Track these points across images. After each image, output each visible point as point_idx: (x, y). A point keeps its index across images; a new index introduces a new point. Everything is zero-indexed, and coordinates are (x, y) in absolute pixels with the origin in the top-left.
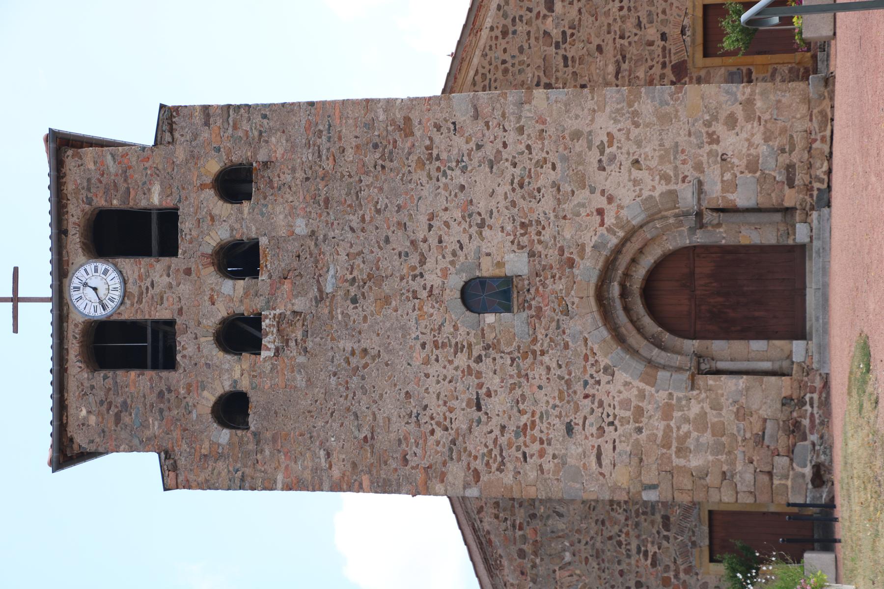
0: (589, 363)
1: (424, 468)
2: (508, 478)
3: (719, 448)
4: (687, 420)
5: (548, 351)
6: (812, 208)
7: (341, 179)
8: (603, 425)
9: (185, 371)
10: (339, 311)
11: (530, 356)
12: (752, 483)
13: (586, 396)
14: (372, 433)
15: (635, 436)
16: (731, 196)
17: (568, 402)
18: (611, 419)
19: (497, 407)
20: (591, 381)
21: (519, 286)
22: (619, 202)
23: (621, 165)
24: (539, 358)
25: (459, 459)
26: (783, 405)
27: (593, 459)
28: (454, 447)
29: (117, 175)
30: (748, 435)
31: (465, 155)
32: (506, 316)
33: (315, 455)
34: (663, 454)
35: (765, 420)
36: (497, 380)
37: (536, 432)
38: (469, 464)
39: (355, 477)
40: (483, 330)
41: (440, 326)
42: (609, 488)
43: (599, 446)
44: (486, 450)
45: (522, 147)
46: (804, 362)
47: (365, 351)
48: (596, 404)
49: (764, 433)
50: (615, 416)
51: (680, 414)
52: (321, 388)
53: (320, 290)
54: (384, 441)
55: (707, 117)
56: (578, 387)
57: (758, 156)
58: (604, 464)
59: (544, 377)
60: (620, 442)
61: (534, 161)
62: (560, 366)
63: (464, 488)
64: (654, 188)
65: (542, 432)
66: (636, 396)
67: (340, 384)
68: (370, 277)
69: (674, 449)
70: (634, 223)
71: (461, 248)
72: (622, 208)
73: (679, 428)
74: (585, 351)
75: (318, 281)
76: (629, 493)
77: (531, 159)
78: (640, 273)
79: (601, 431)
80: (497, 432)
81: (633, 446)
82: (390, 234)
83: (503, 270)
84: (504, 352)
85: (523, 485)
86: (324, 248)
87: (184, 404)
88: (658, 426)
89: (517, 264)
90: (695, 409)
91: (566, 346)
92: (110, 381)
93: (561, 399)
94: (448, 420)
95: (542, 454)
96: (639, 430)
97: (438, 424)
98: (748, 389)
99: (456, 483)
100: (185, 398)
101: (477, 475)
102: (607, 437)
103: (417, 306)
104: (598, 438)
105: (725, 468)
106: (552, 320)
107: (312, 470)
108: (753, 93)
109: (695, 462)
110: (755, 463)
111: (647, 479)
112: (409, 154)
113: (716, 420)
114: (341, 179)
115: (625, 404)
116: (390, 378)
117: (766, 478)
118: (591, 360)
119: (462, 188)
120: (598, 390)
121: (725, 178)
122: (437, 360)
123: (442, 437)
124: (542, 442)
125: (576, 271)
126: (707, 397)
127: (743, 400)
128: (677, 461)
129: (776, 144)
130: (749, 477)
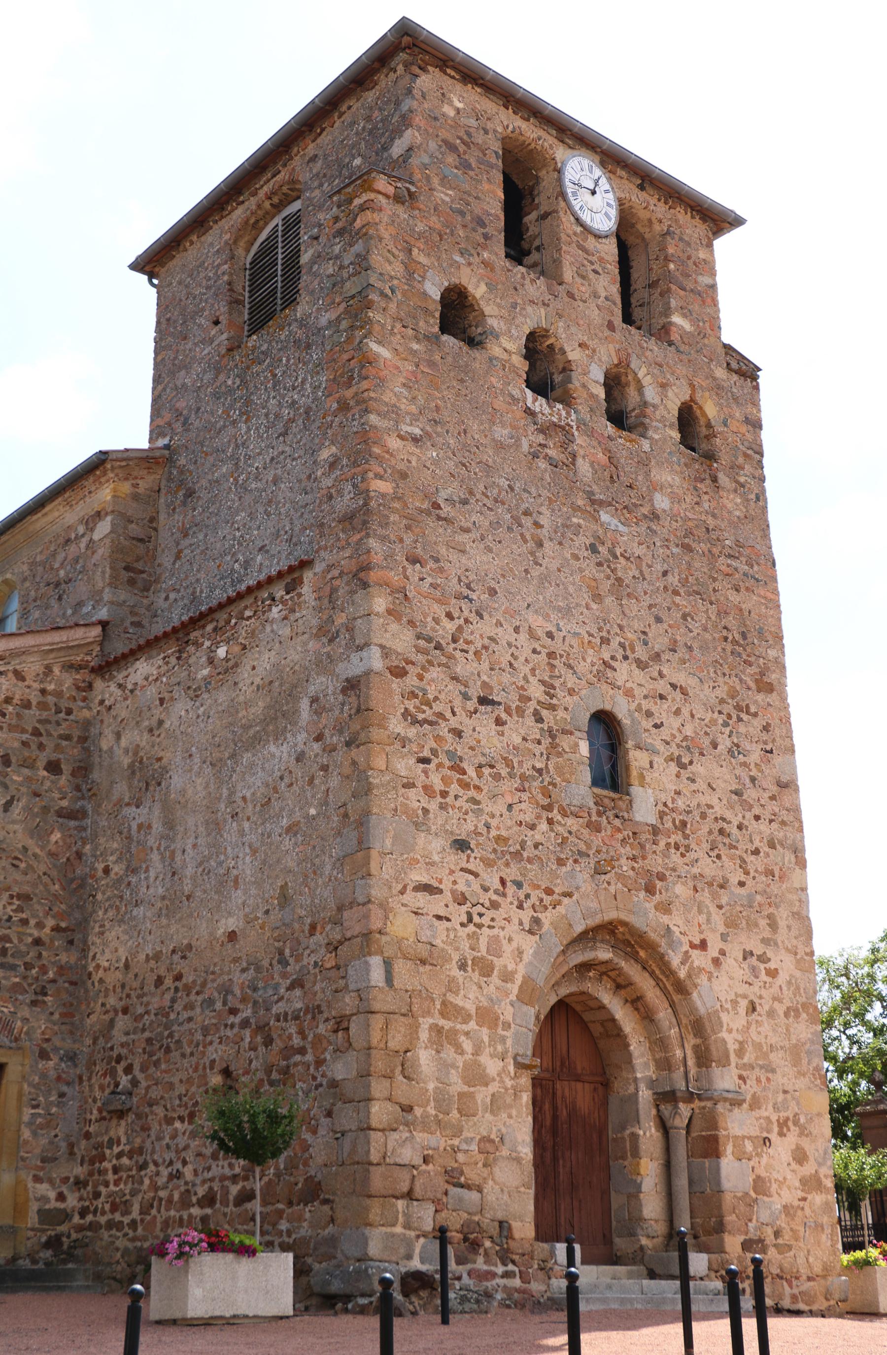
0: (544, 896)
1: (404, 588)
2: (396, 725)
3: (442, 1101)
4: (477, 1052)
5: (552, 830)
7: (711, 577)
8: (469, 904)
9: (509, 270)
10: (581, 521)
11: (545, 802)
12: (399, 1161)
13: (503, 882)
14: (445, 519)
15: (456, 957)
17: (495, 851)
18: (476, 919)
19: (483, 730)
20: (521, 894)
21: (621, 803)
22: (715, 975)
23: (750, 984)
24: (545, 814)
25: (418, 650)
26: (501, 1223)
27: (425, 879)
28: (432, 645)
29: (696, 282)
30: (461, 1157)
31: (745, 759)
32: (587, 777)
33: (415, 419)
34: (433, 1000)
35: (480, 1190)
36: (517, 740)
37: (454, 789)
38: (413, 664)
39: (389, 471)
40: (571, 733)
41: (572, 668)
42: (387, 898)
43: (441, 891)
44: (431, 697)
45: (757, 843)
46: (556, 1263)
47: (540, 544)
48: (495, 897)
49: (462, 1186)
50: (479, 926)
51: (486, 1039)
52: (494, 462)
53: (601, 503)
54: (436, 532)
55: (802, 1120)
56: (512, 872)
57: (770, 1196)
58: (419, 895)
59: (521, 817)
60: (448, 930)
61: (745, 855)
62: (536, 846)
63: (382, 647)
64: (730, 1031)
65: (456, 797)
66: (505, 966)
67: (500, 492)
68: (619, 580)
69: (442, 1022)
70: (695, 995)
71: (656, 726)
73: (467, 1034)
74: (557, 890)
75: (610, 504)
76: (380, 932)
77: (746, 852)
79: (461, 900)
80: (453, 722)
81: (443, 950)
82: (665, 626)
83: (637, 783)
84: (548, 759)
85: (388, 748)
86: (643, 528)
87: (473, 251)
88: (468, 999)
89: (644, 805)
90: (492, 1067)
92: (493, 160)
93: (498, 839)
94: (465, 647)
95: (428, 790)
96: (463, 966)
97: (460, 629)
99: (388, 635)
100: (478, 254)
101: (399, 673)
102: (453, 907)
103: (593, 640)
104: (453, 892)
105: (418, 1111)
106: (589, 846)
107: (395, 406)
108: (827, 1190)
109: (424, 1057)
110: (424, 1167)
111: (401, 967)
112: (741, 680)
113: (479, 1102)
114: (711, 577)
115: (495, 948)
116: (511, 570)
117: (404, 1187)
118: (547, 899)
119: (715, 746)
120: (511, 903)
121: (746, 1141)
122: (534, 651)
123: (444, 629)
124: (444, 794)
125: (642, 894)
126: (506, 1089)
127: (505, 1152)
128: (425, 1023)
129: (782, 1222)
130: (408, 1155)
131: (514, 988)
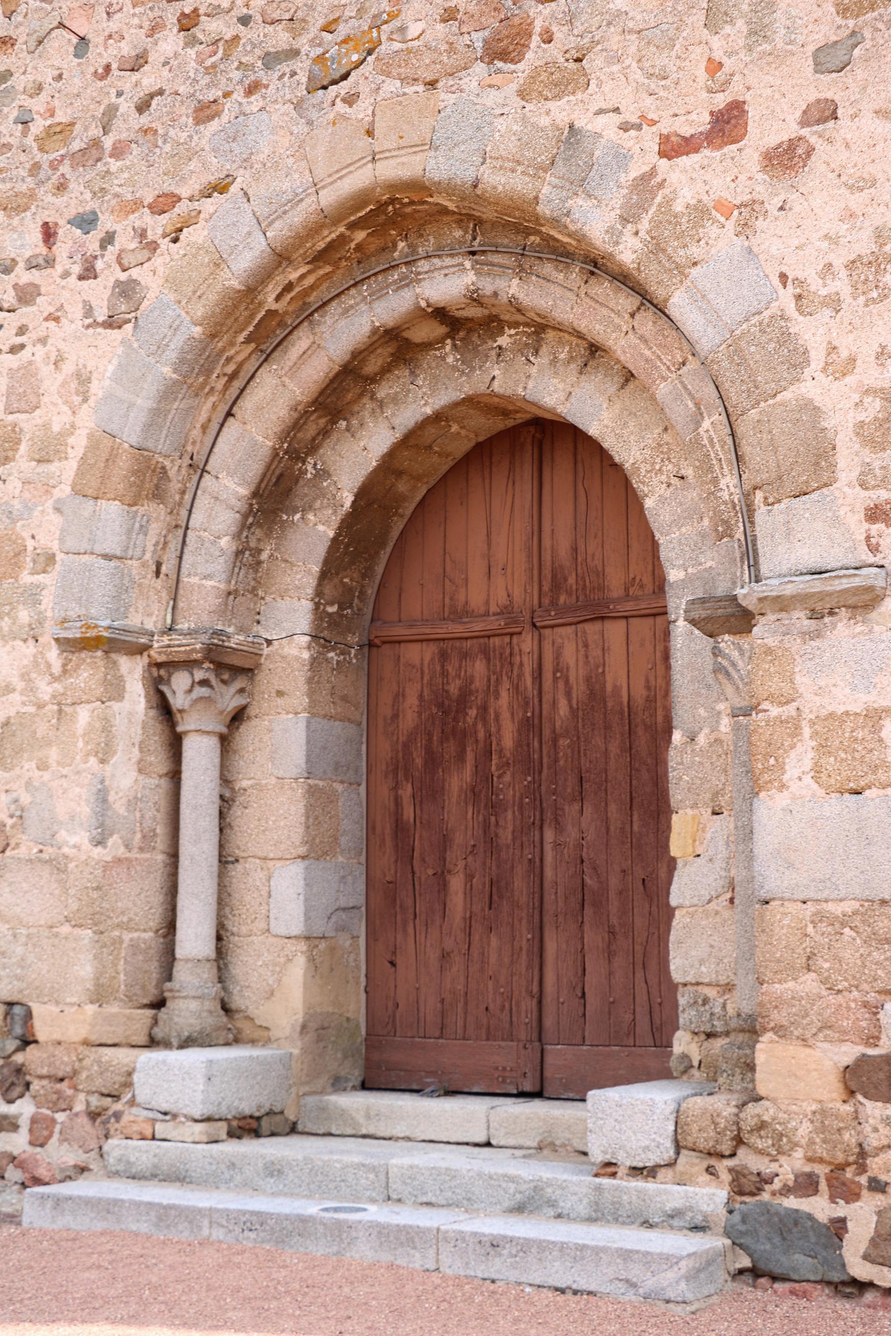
5: (192, 42)
6: (745, 1185)
13: (49, 234)
16: (799, 761)
22: (773, 205)
46: (132, 1102)
72: (745, 228)
78: (551, 387)
91: (206, 112)
98: (58, 866)
118: (157, 225)
120: (66, 274)
126: (40, 706)
131: (66, 470)
